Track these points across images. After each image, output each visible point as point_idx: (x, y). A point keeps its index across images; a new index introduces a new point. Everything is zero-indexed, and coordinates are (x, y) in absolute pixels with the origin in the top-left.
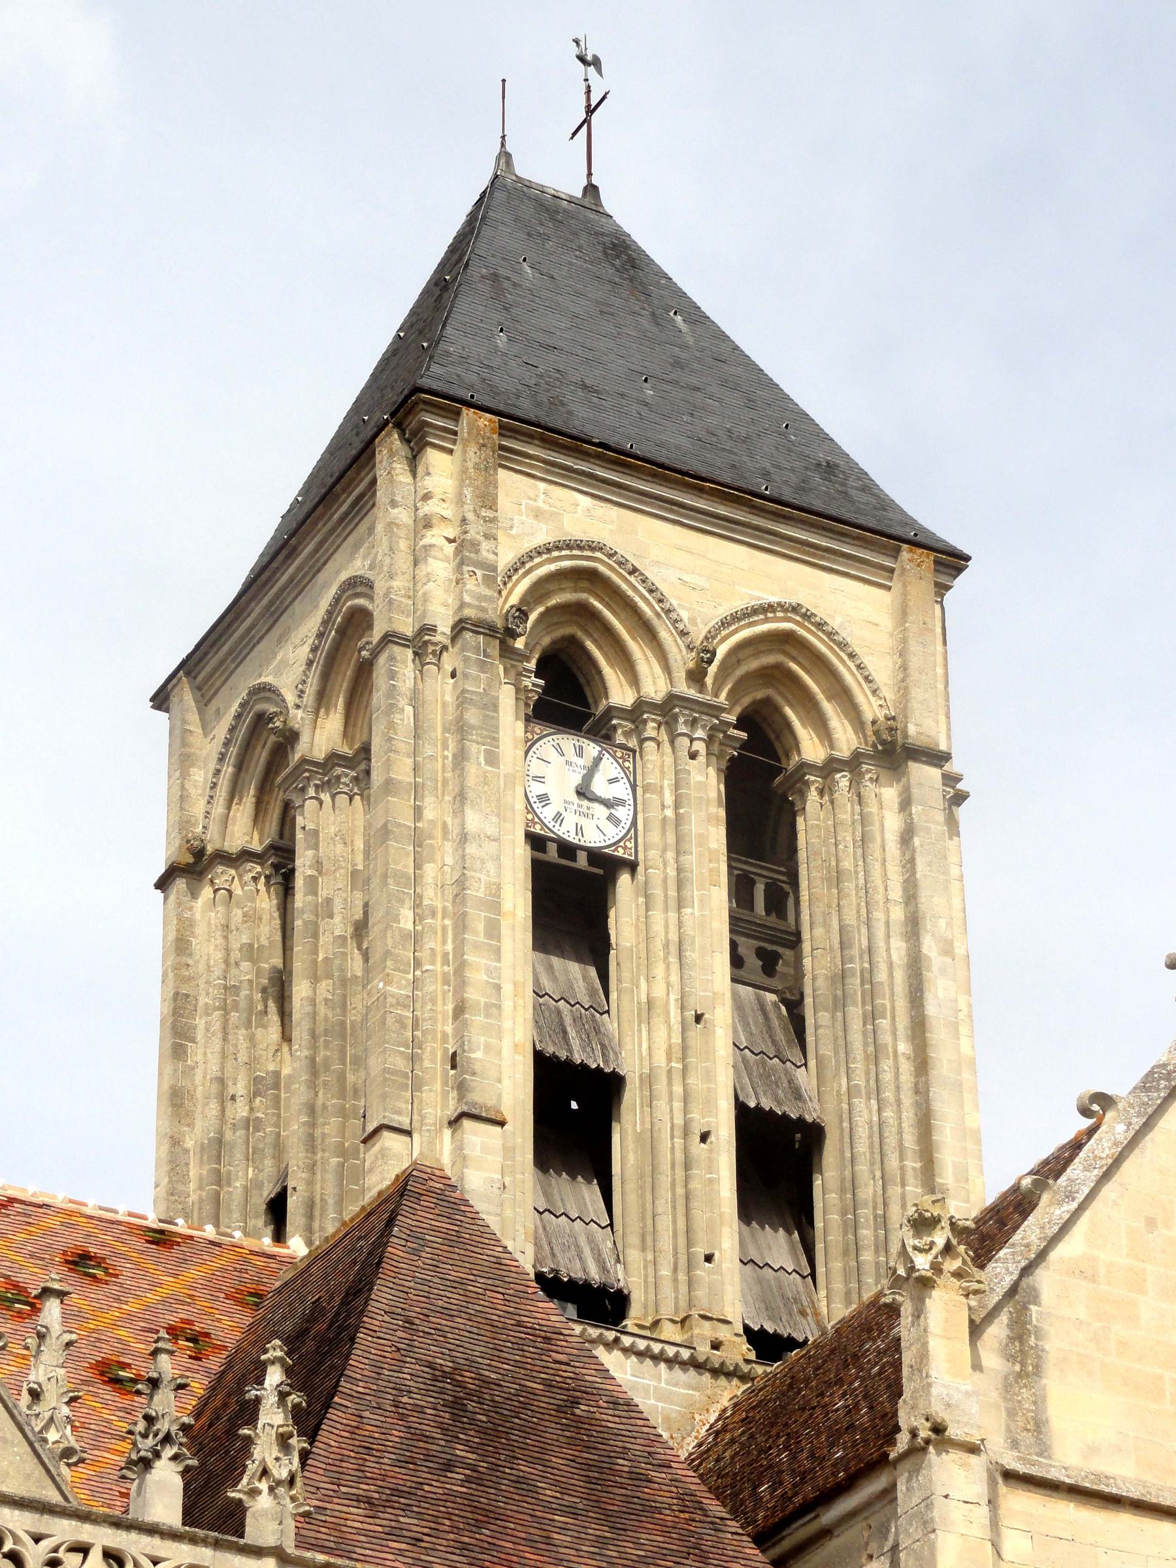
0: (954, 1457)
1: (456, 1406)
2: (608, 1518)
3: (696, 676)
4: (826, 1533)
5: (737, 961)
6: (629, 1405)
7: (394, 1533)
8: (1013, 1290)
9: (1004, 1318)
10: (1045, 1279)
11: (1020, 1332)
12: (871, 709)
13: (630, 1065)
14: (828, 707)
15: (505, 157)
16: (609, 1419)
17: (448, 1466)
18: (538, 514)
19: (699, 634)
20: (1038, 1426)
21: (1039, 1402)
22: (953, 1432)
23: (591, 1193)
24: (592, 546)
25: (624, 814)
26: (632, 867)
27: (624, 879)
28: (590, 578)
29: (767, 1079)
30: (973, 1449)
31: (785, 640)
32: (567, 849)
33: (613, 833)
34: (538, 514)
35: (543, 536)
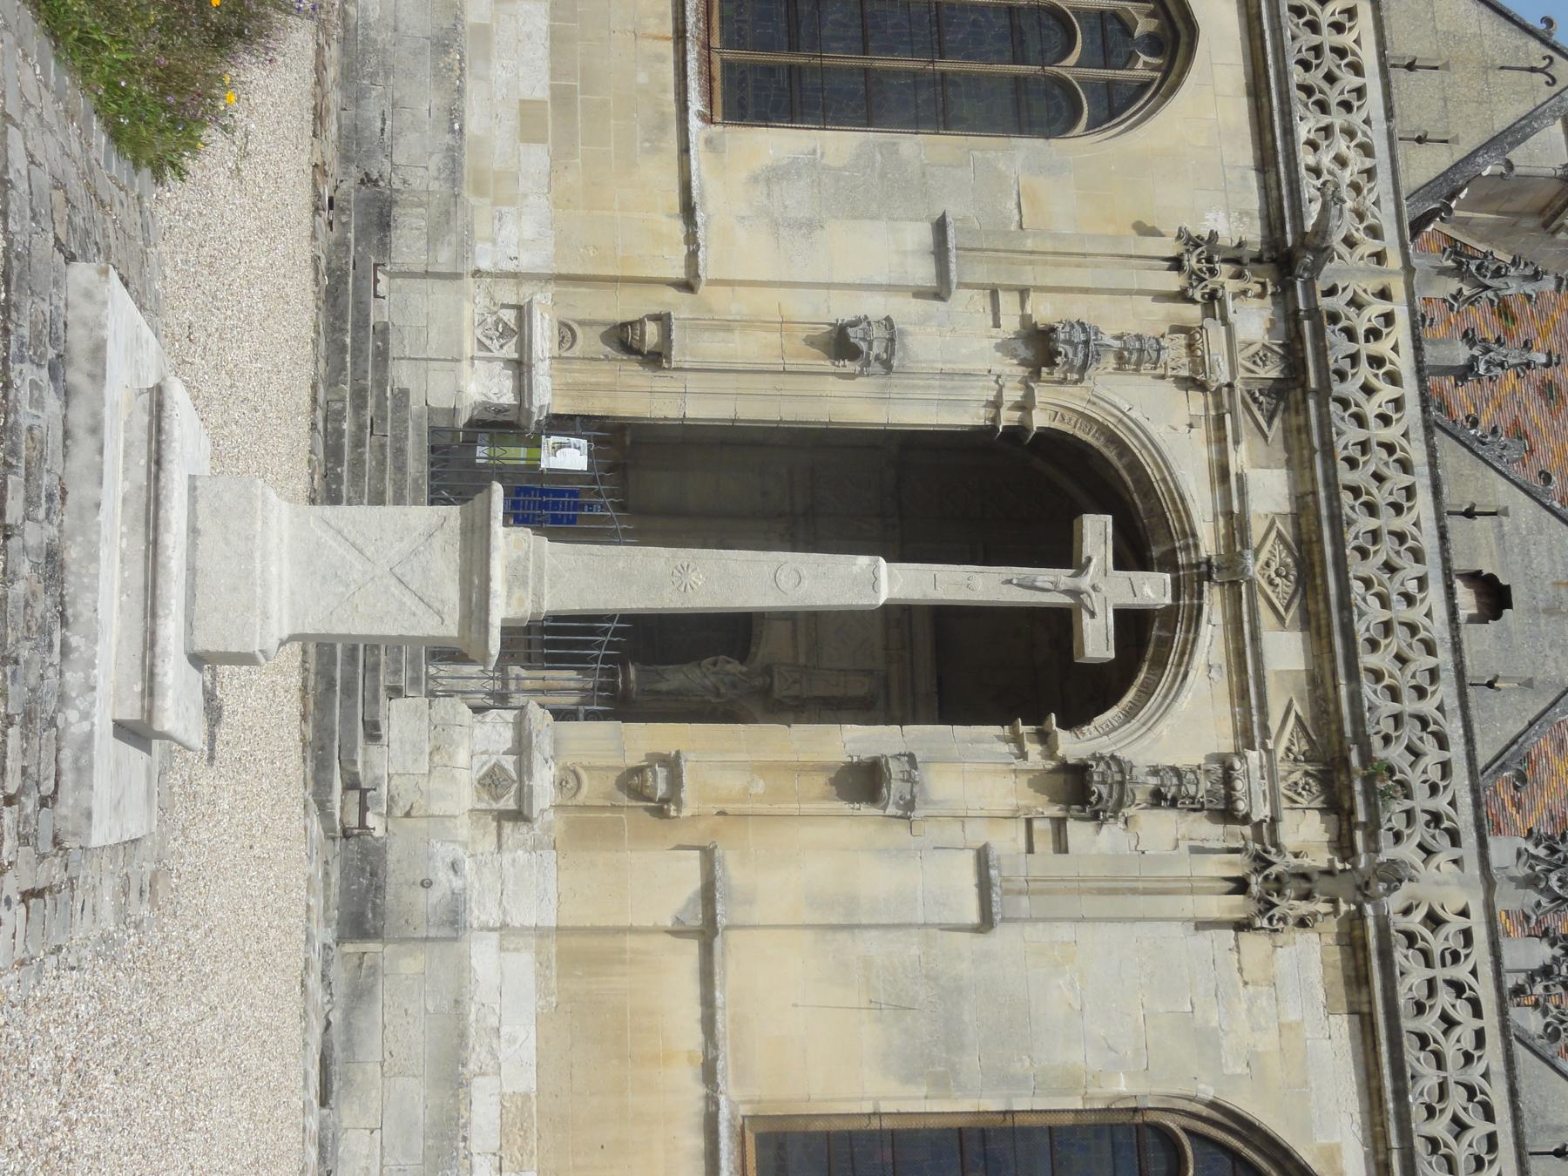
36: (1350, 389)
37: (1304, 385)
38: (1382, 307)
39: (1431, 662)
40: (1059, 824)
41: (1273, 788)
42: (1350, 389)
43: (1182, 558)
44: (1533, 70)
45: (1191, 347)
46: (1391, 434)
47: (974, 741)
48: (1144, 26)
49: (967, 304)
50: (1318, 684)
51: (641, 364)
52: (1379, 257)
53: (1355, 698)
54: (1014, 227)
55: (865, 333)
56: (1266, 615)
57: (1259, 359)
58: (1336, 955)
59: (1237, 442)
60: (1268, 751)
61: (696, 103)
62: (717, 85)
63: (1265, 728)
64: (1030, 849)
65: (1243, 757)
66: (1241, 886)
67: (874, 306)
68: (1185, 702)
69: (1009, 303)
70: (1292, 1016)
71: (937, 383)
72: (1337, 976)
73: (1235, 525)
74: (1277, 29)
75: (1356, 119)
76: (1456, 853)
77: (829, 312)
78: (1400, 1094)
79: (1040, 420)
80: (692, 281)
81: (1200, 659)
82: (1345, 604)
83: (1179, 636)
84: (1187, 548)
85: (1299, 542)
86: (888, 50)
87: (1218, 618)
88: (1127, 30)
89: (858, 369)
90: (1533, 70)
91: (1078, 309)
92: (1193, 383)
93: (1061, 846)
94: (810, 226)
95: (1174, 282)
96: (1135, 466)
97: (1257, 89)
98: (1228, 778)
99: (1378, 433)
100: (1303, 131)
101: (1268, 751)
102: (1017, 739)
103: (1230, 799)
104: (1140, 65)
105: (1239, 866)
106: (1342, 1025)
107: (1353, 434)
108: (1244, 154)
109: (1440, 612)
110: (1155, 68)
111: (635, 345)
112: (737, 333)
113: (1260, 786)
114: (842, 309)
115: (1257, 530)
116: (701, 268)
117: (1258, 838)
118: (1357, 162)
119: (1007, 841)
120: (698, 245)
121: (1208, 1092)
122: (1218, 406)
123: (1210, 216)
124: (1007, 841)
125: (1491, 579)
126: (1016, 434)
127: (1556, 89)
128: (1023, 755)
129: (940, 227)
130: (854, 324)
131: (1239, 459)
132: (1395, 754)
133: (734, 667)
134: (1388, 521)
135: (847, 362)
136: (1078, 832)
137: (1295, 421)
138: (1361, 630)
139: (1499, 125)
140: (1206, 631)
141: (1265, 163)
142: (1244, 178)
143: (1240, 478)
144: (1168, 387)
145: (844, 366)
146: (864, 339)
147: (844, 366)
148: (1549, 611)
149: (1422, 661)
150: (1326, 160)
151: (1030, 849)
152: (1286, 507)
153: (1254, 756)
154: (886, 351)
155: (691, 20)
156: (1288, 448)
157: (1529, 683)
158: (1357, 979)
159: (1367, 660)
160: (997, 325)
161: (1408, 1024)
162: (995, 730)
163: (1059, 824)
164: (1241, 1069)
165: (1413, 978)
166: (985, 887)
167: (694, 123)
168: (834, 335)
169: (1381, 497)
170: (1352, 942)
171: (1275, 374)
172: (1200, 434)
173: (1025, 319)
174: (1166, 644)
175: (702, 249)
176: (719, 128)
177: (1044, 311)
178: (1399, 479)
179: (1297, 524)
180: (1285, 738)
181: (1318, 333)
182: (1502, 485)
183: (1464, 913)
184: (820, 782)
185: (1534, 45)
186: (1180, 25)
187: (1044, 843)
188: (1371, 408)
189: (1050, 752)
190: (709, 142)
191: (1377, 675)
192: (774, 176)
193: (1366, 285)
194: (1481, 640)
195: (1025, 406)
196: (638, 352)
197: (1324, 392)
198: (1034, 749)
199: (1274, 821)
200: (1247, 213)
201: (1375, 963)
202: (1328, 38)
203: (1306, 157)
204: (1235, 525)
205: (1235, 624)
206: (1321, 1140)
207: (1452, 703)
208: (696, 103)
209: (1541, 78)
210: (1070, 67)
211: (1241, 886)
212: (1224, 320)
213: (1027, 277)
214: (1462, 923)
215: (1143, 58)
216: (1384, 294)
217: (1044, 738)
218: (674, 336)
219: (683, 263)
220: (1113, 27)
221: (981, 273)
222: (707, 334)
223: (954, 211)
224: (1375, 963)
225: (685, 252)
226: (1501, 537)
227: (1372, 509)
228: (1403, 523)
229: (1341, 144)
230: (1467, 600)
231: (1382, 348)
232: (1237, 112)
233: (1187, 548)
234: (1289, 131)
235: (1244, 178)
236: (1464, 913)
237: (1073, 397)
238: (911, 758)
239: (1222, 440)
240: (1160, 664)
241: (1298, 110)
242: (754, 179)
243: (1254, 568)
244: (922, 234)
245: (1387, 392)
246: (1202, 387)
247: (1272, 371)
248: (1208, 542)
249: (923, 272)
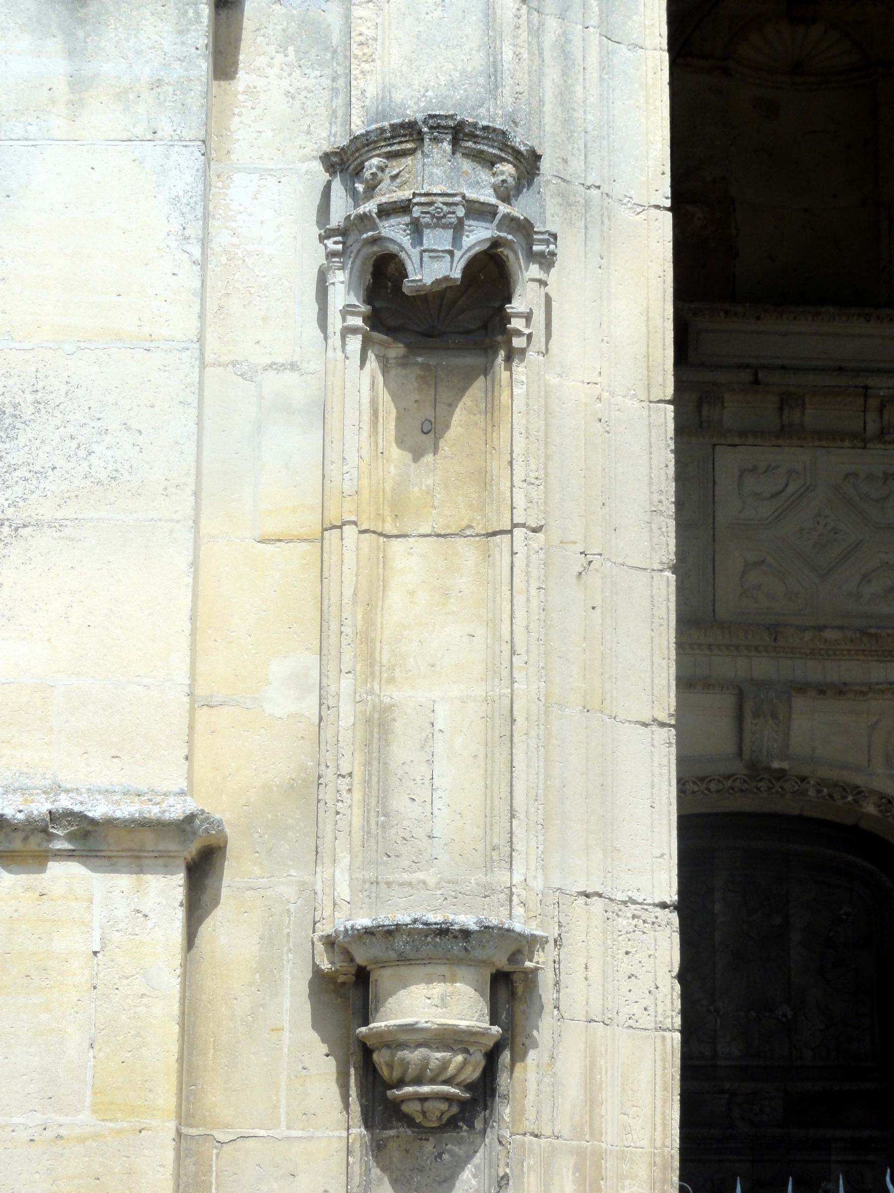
51: (518, 1057)
55: (439, 222)
71: (552, 24)
77: (293, 366)
80: (192, 849)
89: (534, 270)
111: (473, 1073)
112: (392, 694)
116: (154, 811)
120: (54, 817)
135: (517, 305)
145: (528, 317)
146: (458, 228)
147: (528, 317)
154: (490, 162)
168: (397, 350)
175: (65, 803)
196: (492, 1057)
218: (467, 920)
219: (123, 881)
222: (399, 803)
225: (75, 869)
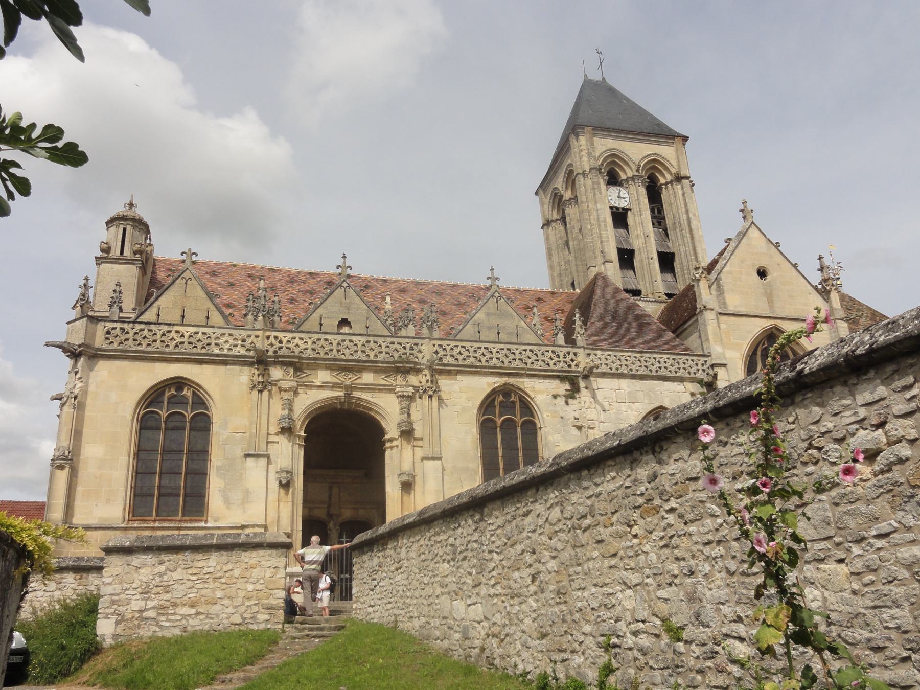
0: (709, 312)
1: (612, 316)
2: (643, 332)
3: (638, 171)
4: (686, 329)
5: (653, 224)
6: (644, 311)
7: (604, 340)
8: (716, 278)
9: (715, 284)
10: (722, 275)
11: (719, 286)
12: (673, 171)
13: (635, 247)
14: (664, 172)
15: (586, 75)
16: (641, 314)
17: (612, 327)
18: (602, 145)
19: (637, 163)
20: (725, 303)
21: (724, 299)
22: (708, 307)
23: (632, 272)
24: (614, 149)
25: (627, 200)
26: (630, 209)
27: (629, 212)
28: (614, 155)
29: (662, 245)
30: (712, 310)
31: (654, 160)
32: (618, 208)
33: (626, 204)
34: (602, 145)
35: (604, 149)
36: (297, 350)
37: (296, 362)
38: (272, 339)
39: (372, 342)
40: (416, 439)
41: (405, 386)
42: (297, 350)
43: (343, 401)
44: (186, 283)
45: (285, 391)
46: (310, 342)
47: (391, 458)
48: (173, 392)
49: (273, 450)
50: (377, 371)
52: (257, 336)
53: (382, 362)
54: (245, 435)
56: (358, 381)
57: (287, 373)
58: (443, 377)
59: (313, 382)
60: (396, 385)
61: (202, 524)
62: (193, 518)
63: (389, 386)
64: (422, 447)
65: (398, 392)
66: (430, 397)
67: (273, 477)
68: (381, 404)
69: (271, 439)
70: (458, 389)
72: (448, 377)
73: (335, 386)
74: (182, 354)
75: (213, 336)
76: (420, 345)
78: (477, 367)
79: (302, 433)
81: (371, 399)
82: (358, 361)
83: (364, 404)
84: (340, 399)
85: (338, 370)
86: (181, 467)
87: (360, 393)
88: (173, 396)
90: (186, 283)
91: (273, 420)
92: (296, 393)
93: (421, 439)
94: (247, 492)
95: (266, 393)
96: (316, 410)
97: (201, 362)
98: (403, 396)
99: (310, 345)
100: (217, 351)
101: (396, 385)
102: (391, 448)
103: (408, 396)
104: (188, 394)
105: (425, 397)
106: (459, 378)
107: (309, 351)
108: (222, 368)
109: (359, 338)
110: (188, 389)
113: (405, 389)
114: (274, 485)
115: (335, 380)
117: (418, 391)
118: (226, 338)
119: (419, 453)
121: (476, 411)
122: (301, 386)
123: (241, 380)
124: (419, 453)
125: (339, 322)
126: (306, 440)
127: (193, 278)
128: (397, 446)
129: (248, 456)
130: (280, 482)
131: (318, 382)
132: (396, 355)
133: (331, 525)
134: (335, 347)
136: (417, 434)
137: (305, 366)
138: (364, 358)
139: (205, 296)
140: (363, 397)
141: (225, 363)
142: (229, 369)
143: (323, 383)
144: (296, 399)
148: (348, 309)
149: (372, 344)
150: (227, 346)
151: (422, 447)
152: (329, 372)
153: (398, 389)
155: (172, 525)
156: (313, 369)
157: (367, 318)
158: (449, 372)
159: (372, 358)
160: (278, 442)
161: (460, 363)
162: (388, 453)
163: (416, 439)
164: (470, 402)
165: (448, 360)
166: (433, 459)
167: (209, 525)
169: (328, 348)
170: (441, 372)
171: (292, 370)
172: (308, 391)
173: (277, 434)
174: (364, 407)
176: (209, 519)
177: (274, 429)
178: (322, 342)
179: (334, 370)
180: (390, 381)
181: (282, 356)
182: (314, 315)
183: (434, 345)
184: (405, 498)
185: (178, 281)
186: (176, 381)
187: (420, 443)
188: (303, 346)
189: (396, 439)
190: (215, 521)
191: (376, 356)
192: (227, 502)
193: (267, 343)
194: (357, 328)
195: (299, 436)
197: (300, 358)
198: (395, 443)
199: (413, 387)
200: (241, 371)
201: (446, 368)
202: (186, 340)
203: (226, 352)
204: (335, 386)
205: (362, 390)
206: (485, 386)
207: (383, 339)
208: (202, 524)
209: (189, 282)
210: (189, 415)
211: (430, 397)
212: (279, 381)
213: (264, 432)
214: (436, 346)
215: (185, 392)
216: (268, 338)
217: (390, 440)
220: (172, 400)
221: (263, 446)
223: (239, 453)
224: (446, 368)
226: (328, 318)
227: (331, 350)
228: (335, 343)
229: (221, 341)
230: (346, 330)
231: (285, 340)
232: (208, 369)
233: (340, 399)
234: (217, 355)
235: (229, 369)
236: (434, 345)
237: (298, 424)
238: (400, 475)
239: (311, 386)
240: (370, 409)
241: (210, 352)
242: (228, 508)
243: (348, 382)
244: (250, 461)
245: (297, 341)
246: (297, 389)
247: (292, 371)
248: (340, 393)
249: (263, 461)
